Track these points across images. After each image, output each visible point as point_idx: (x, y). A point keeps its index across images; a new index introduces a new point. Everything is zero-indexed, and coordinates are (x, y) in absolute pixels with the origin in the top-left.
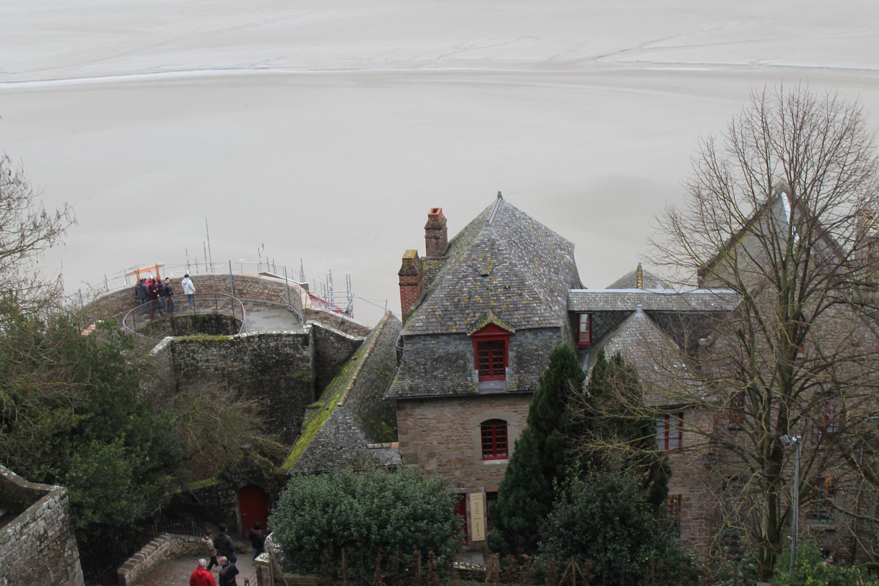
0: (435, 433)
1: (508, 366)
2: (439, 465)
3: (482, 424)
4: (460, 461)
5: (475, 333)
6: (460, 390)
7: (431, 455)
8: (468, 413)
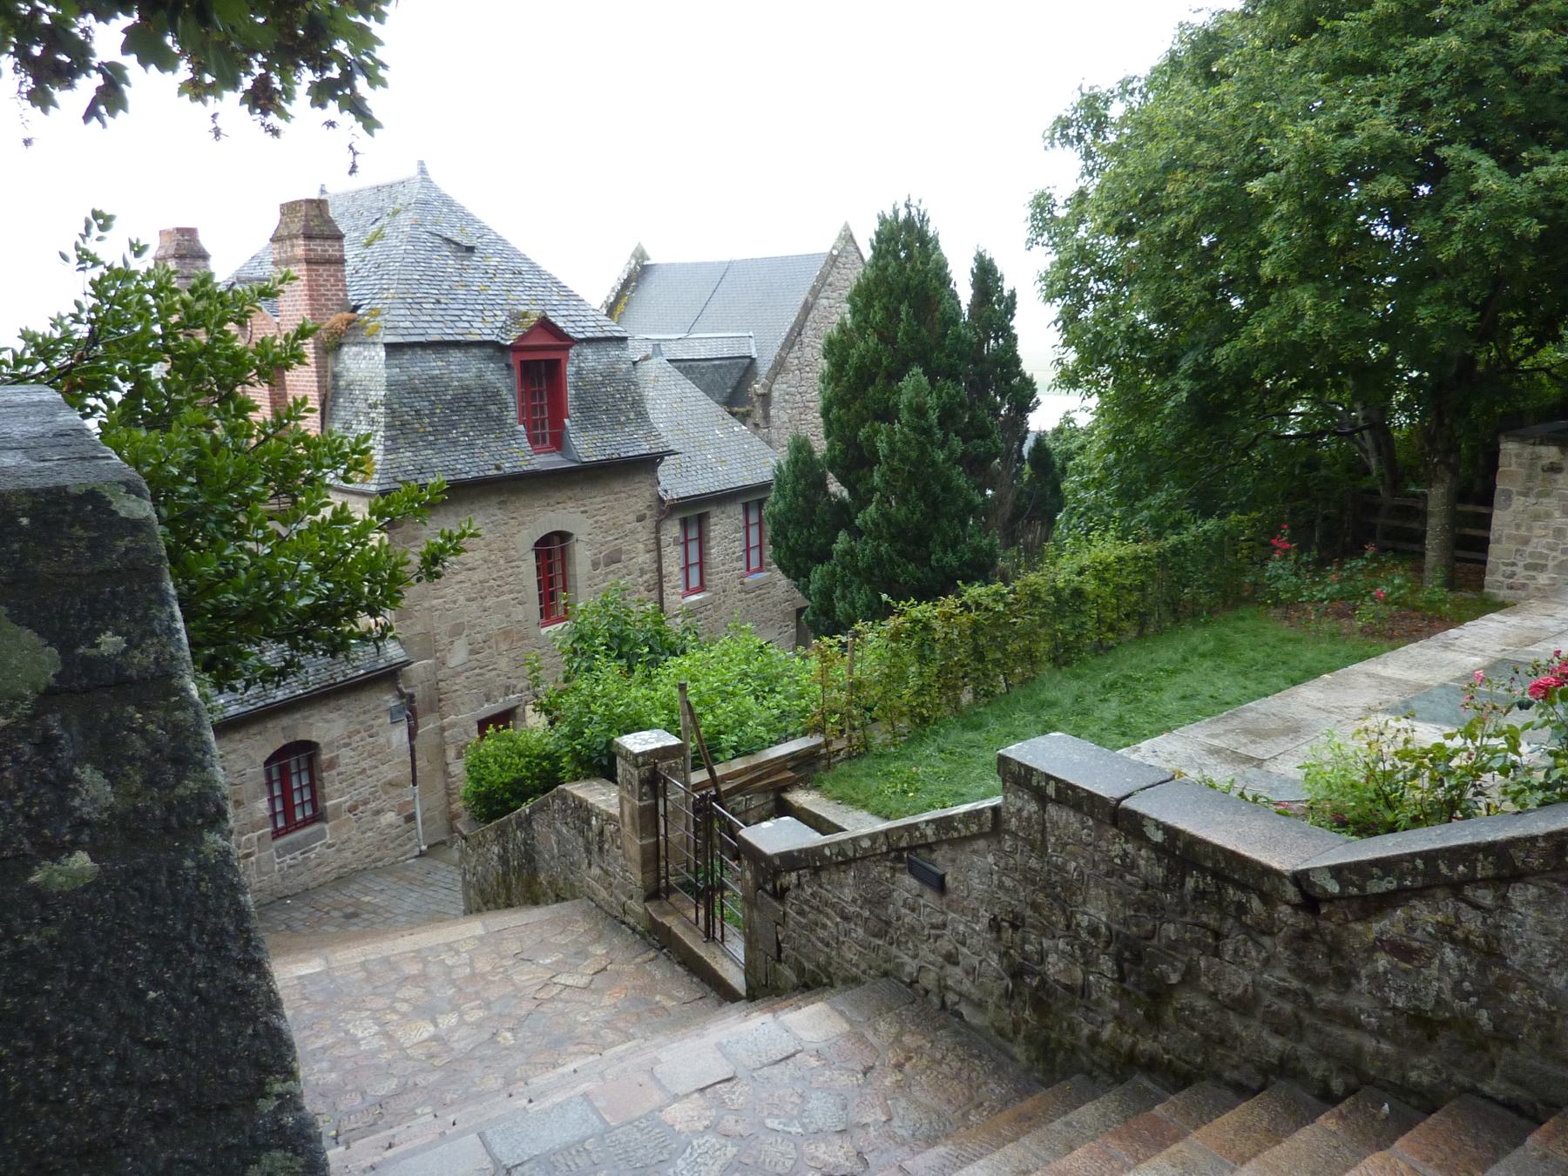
2: (473, 652)
3: (537, 544)
4: (506, 634)
5: (521, 338)
6: (507, 467)
7: (457, 631)
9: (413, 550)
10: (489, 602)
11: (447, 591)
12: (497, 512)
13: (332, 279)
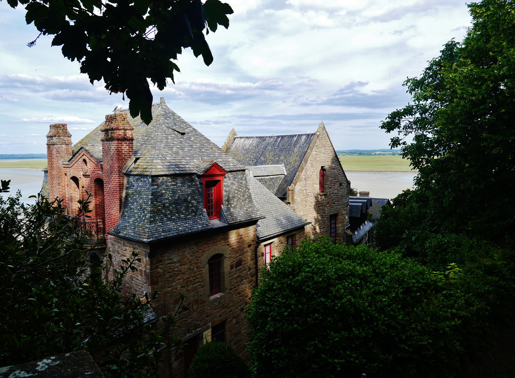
0: (179, 277)
1: (223, 204)
3: (209, 260)
8: (200, 251)
9: (160, 266)
10: (190, 288)
11: (174, 284)
12: (194, 247)
13: (127, 147)
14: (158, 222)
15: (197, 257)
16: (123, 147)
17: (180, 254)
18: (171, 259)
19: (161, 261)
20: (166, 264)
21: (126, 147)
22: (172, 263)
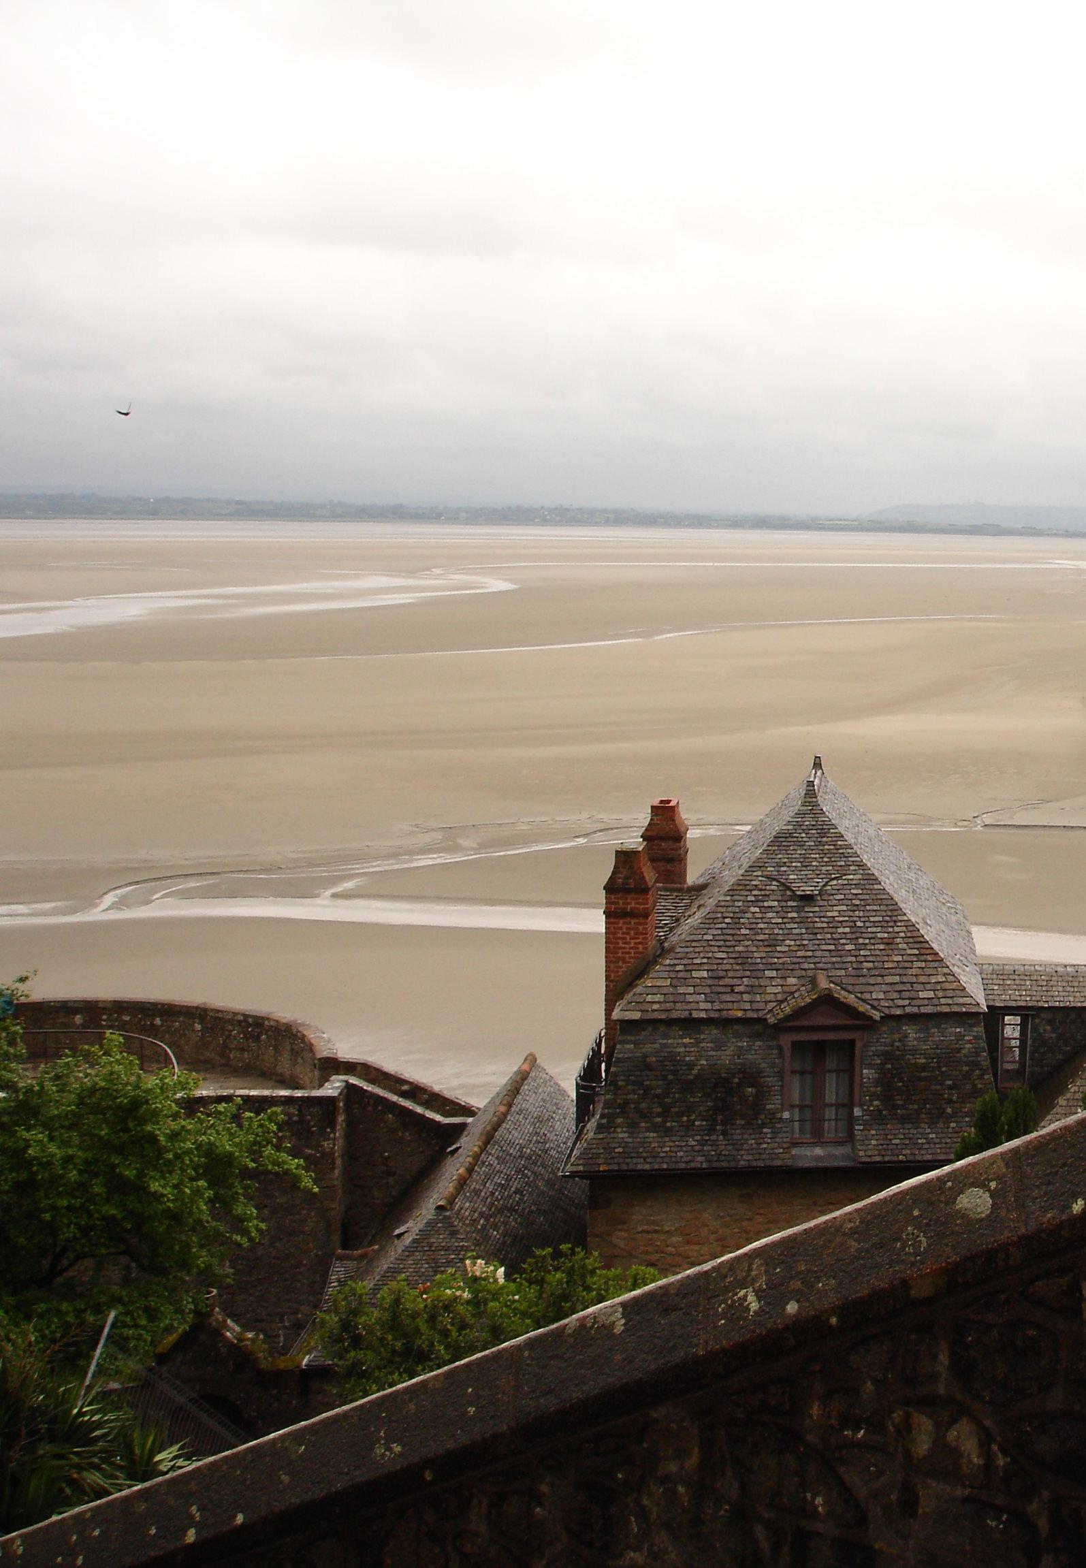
8: (760, 1218)
14: (619, 1130)
15: (746, 1232)
16: (620, 932)
17: (689, 1216)
18: (654, 1222)
19: (624, 1222)
20: (639, 1233)
21: (628, 934)
22: (656, 1232)
